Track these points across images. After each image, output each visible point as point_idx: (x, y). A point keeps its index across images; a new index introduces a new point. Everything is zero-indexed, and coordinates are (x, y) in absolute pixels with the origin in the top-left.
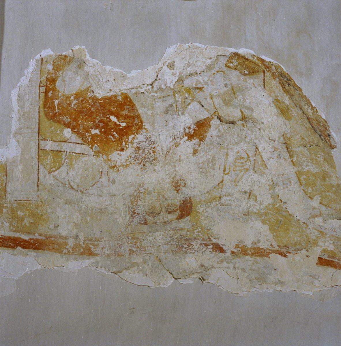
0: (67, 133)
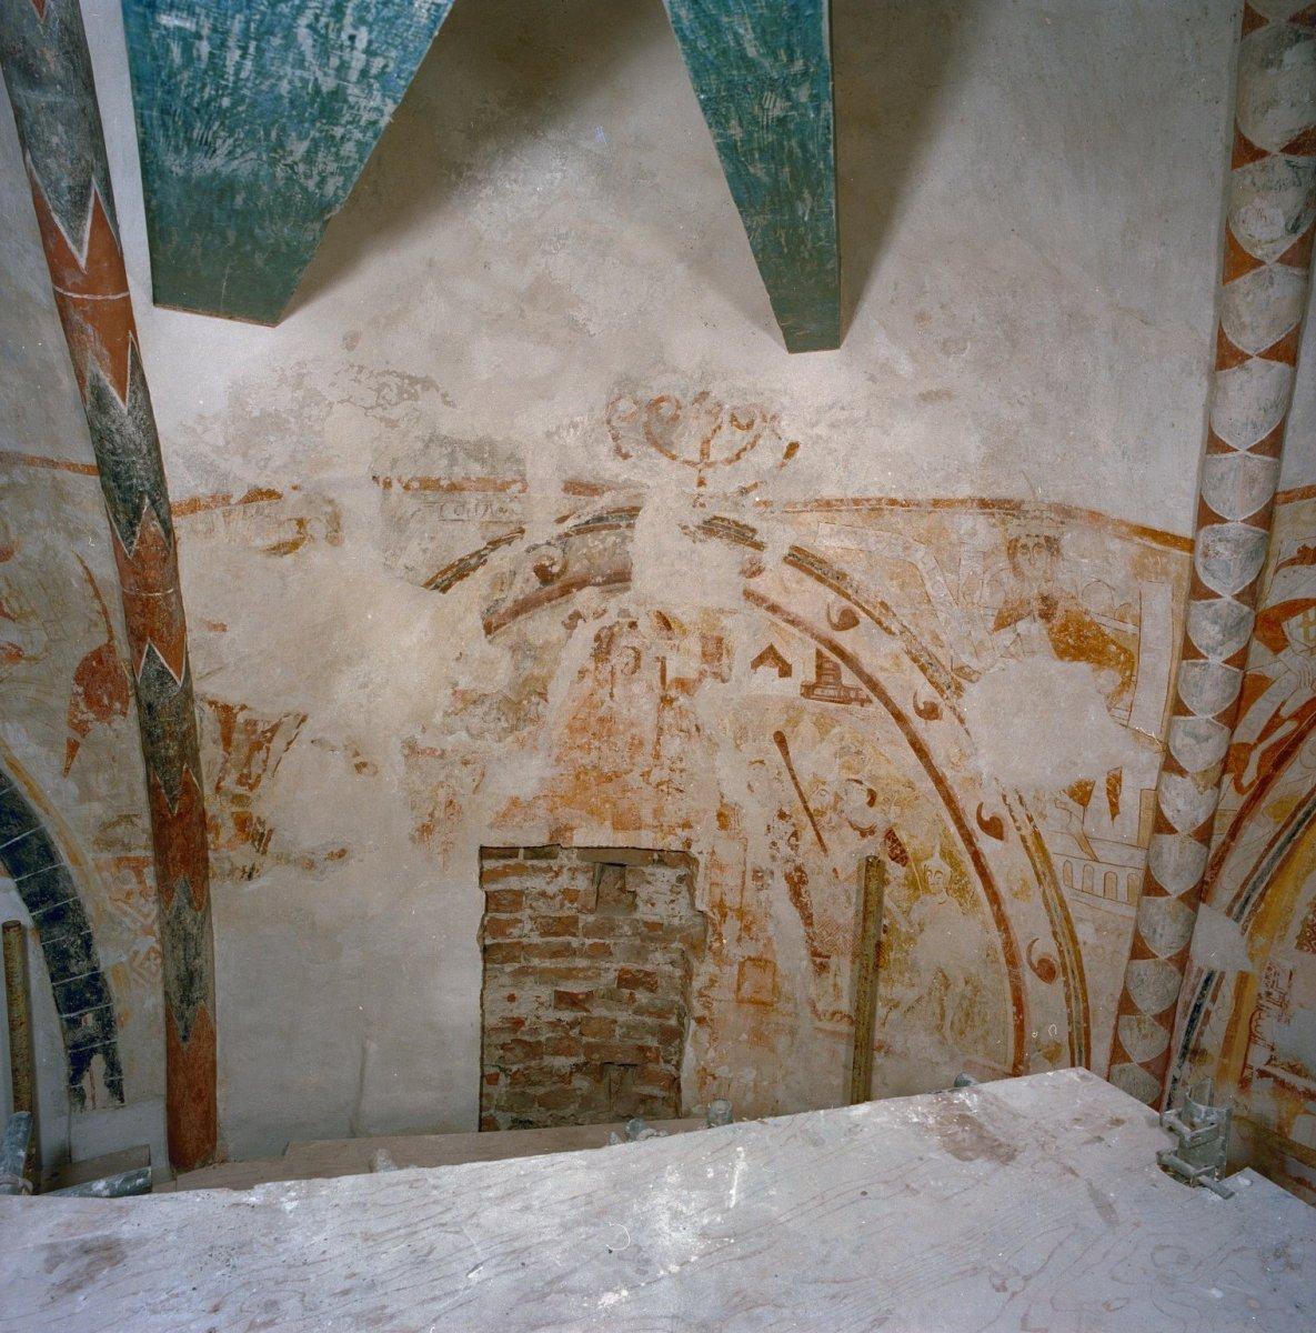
0: (1112, 636)
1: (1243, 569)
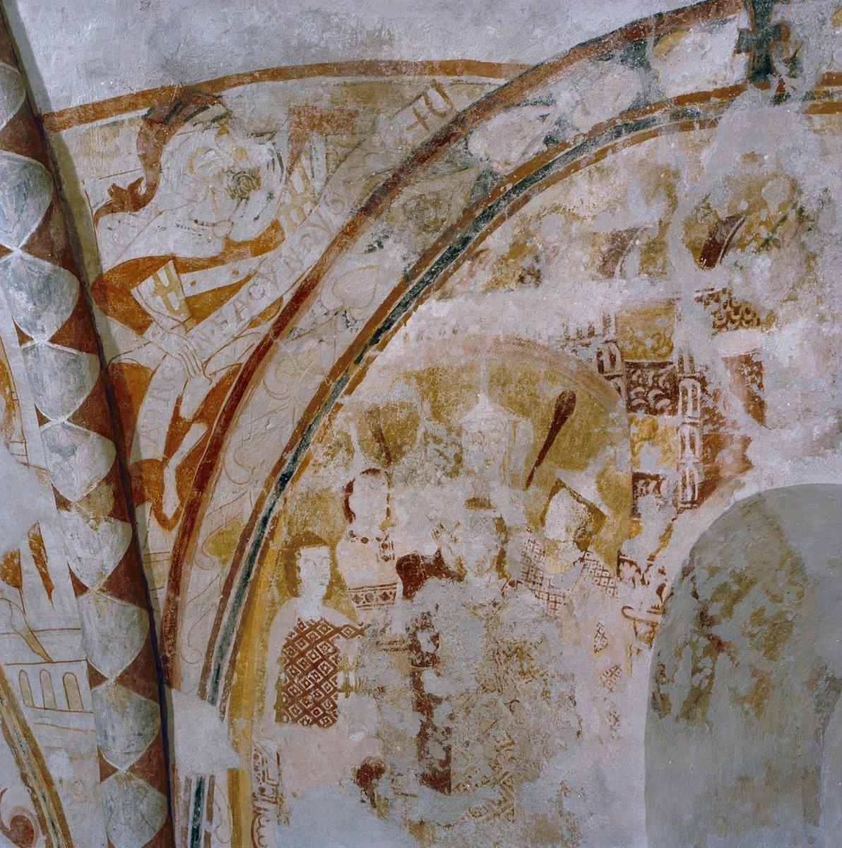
1: (19, 211)
